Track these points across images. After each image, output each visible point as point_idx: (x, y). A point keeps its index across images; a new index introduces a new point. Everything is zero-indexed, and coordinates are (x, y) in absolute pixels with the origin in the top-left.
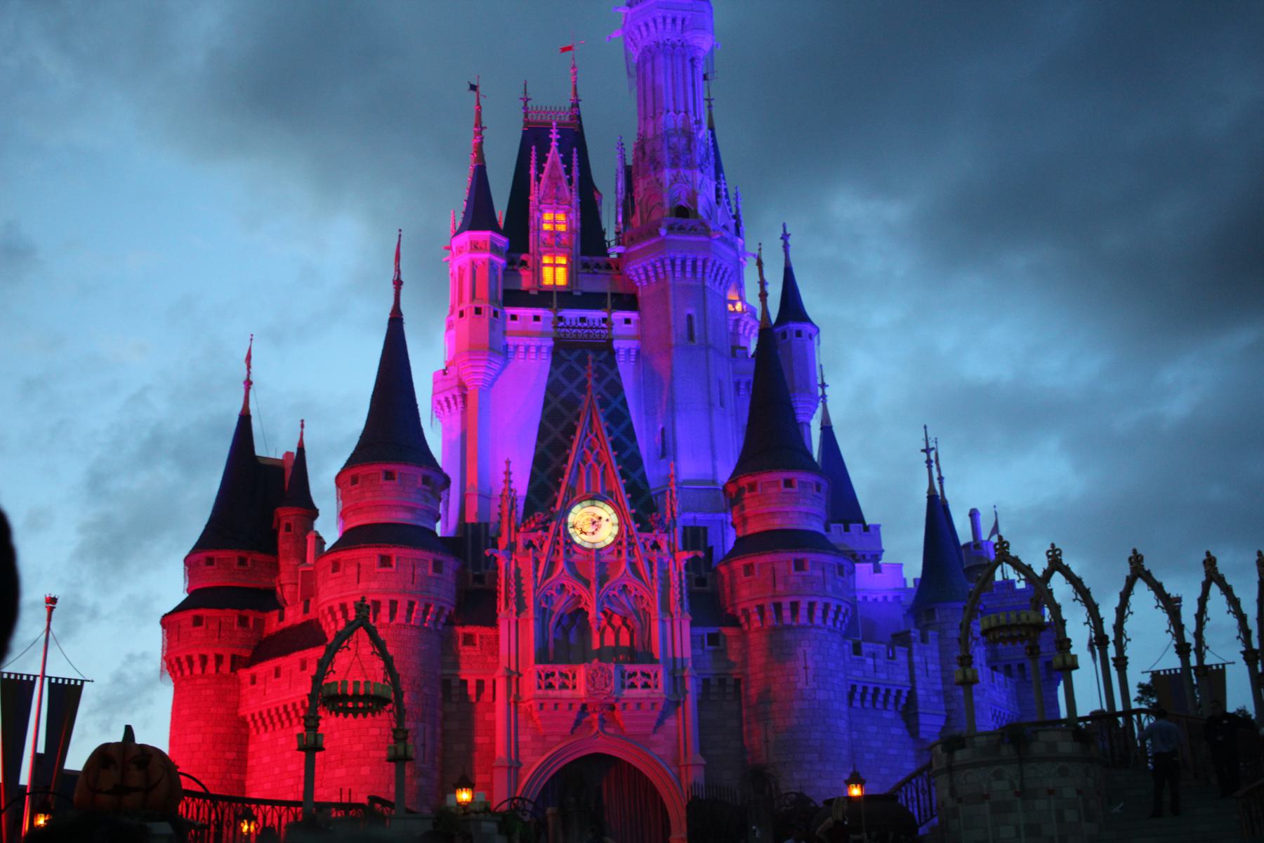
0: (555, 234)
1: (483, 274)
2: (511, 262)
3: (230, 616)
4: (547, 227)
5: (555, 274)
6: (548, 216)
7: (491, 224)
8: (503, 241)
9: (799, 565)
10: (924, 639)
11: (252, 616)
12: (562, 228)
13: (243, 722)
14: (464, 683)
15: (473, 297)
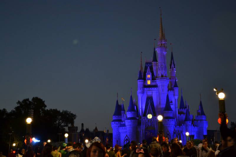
0: (149, 78)
1: (141, 84)
2: (144, 82)
3: (118, 122)
4: (148, 77)
5: (149, 82)
6: (148, 76)
7: (142, 79)
8: (143, 81)
9: (168, 120)
10: (184, 125)
11: (120, 122)
12: (150, 77)
13: (119, 132)
14: (139, 131)
15: (140, 87)
